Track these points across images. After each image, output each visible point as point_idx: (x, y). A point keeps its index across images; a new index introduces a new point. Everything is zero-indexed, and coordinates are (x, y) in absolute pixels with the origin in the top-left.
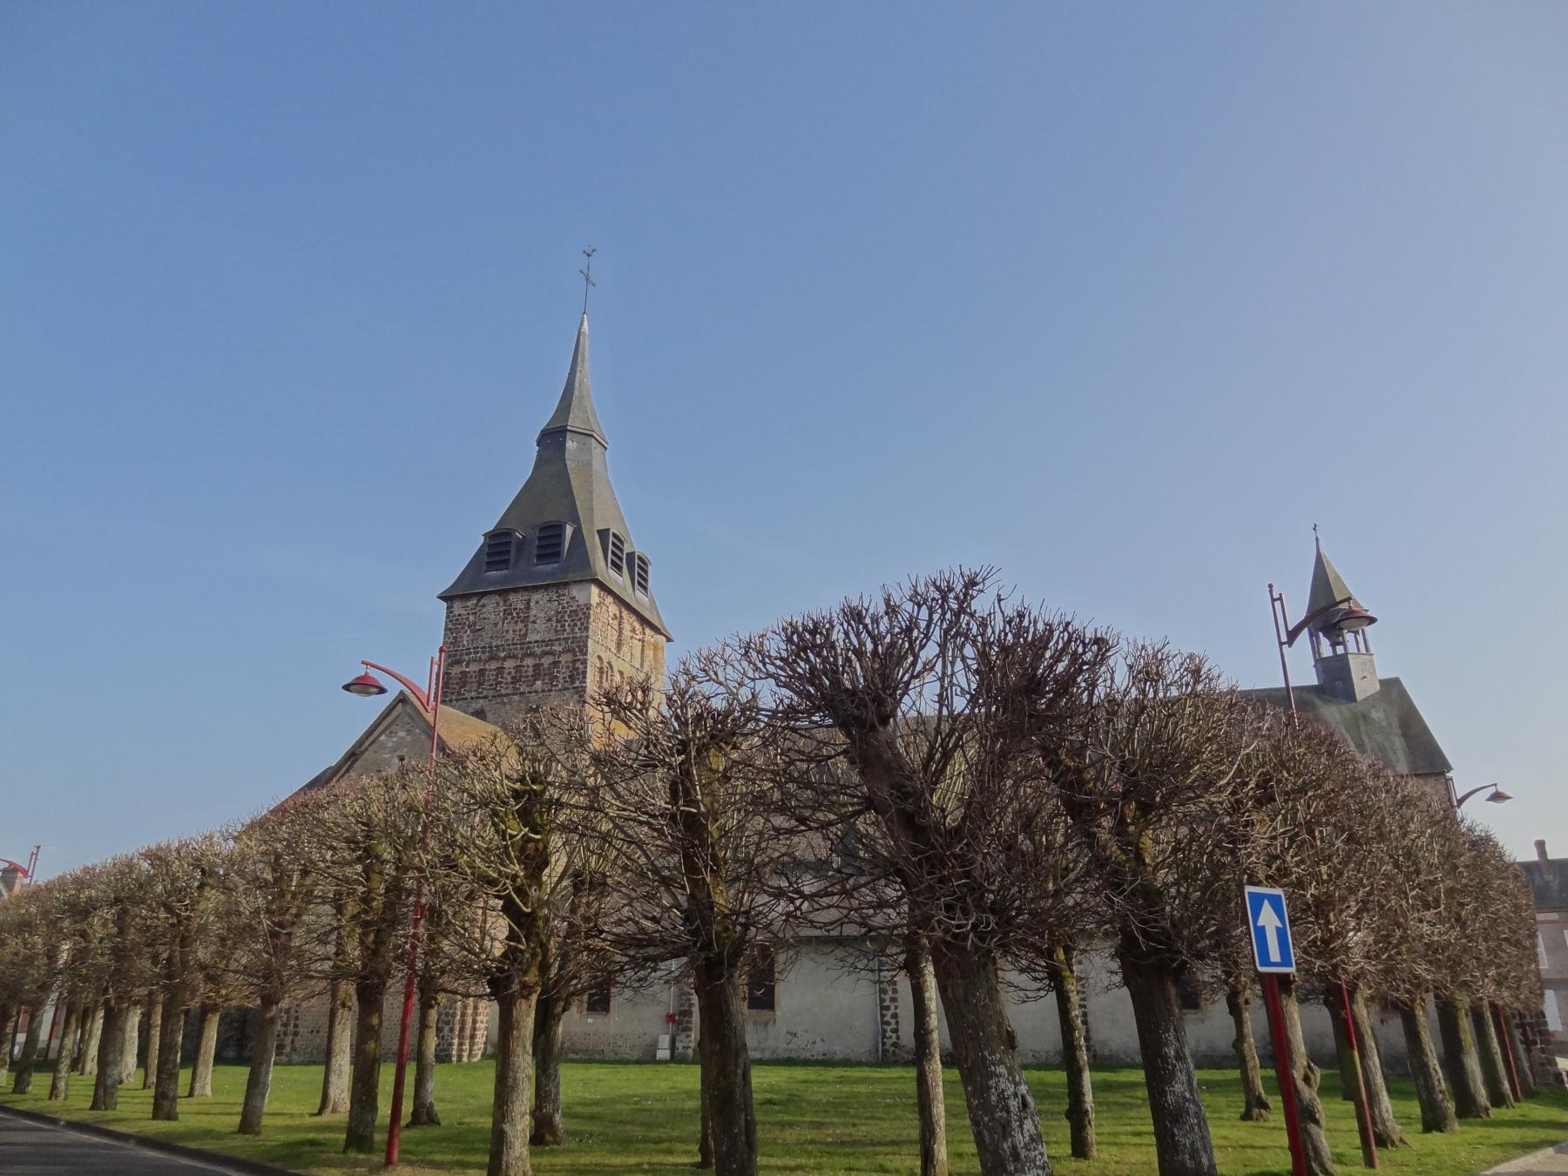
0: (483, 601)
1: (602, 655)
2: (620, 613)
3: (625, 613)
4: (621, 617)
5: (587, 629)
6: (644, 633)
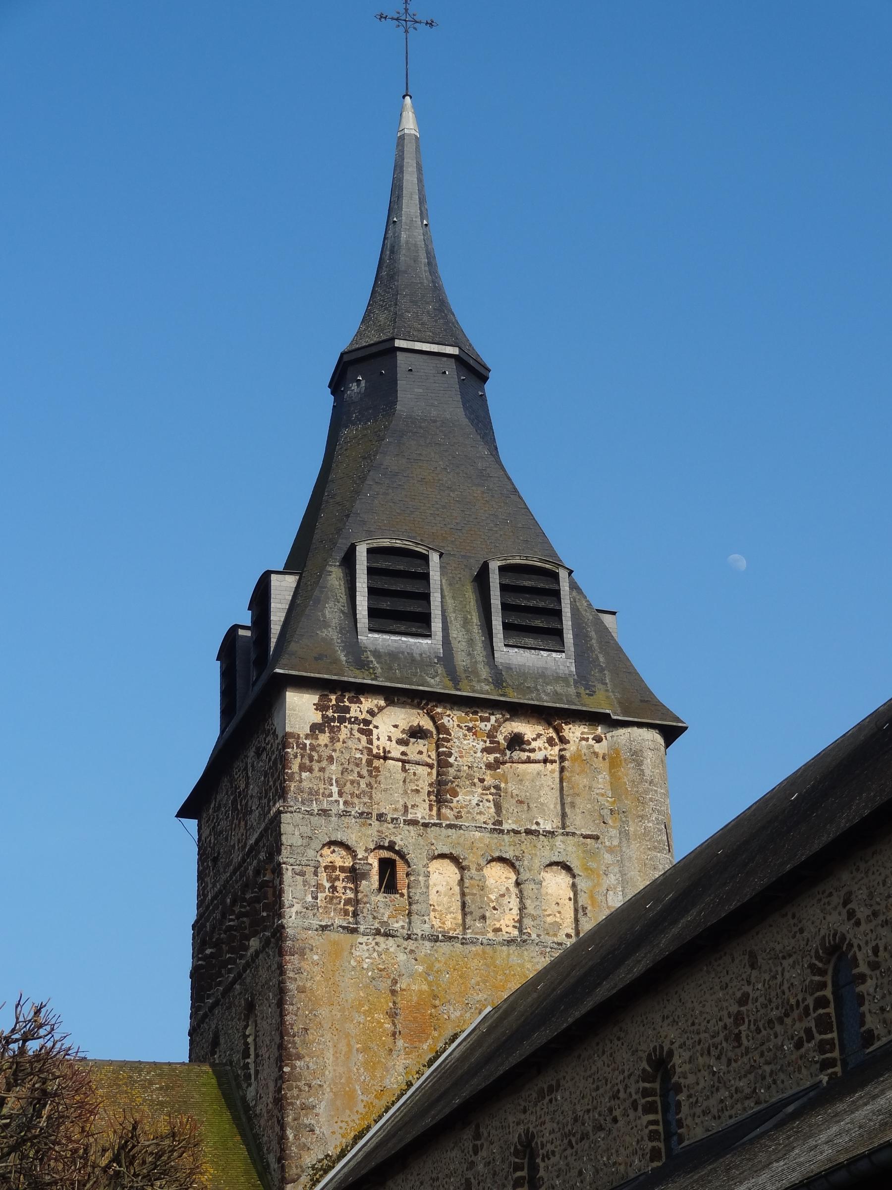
0: (219, 798)
1: (351, 838)
2: (433, 719)
3: (452, 719)
4: (441, 729)
5: (282, 793)
6: (563, 740)
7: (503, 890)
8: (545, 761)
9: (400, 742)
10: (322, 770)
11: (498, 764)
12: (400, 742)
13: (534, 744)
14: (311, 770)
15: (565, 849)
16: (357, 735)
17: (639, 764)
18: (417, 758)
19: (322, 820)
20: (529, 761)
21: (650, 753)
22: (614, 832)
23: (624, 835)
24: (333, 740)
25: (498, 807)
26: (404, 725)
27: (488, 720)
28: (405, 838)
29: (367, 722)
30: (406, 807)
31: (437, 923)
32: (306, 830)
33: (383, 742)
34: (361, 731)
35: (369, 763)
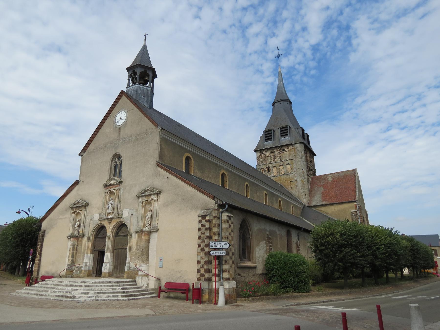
7: (282, 169)
8: (287, 151)
9: (269, 154)
10: (260, 160)
11: (280, 153)
12: (269, 154)
13: (286, 150)
14: (259, 160)
15: (288, 162)
16: (264, 155)
17: (297, 148)
18: (272, 155)
19: (261, 166)
20: (285, 152)
21: (298, 147)
22: (295, 158)
23: (296, 158)
24: (261, 156)
25: (281, 159)
26: (270, 152)
27: (279, 148)
28: (270, 166)
29: (265, 153)
30: (271, 162)
31: (274, 174)
32: (259, 168)
33: (268, 155)
34: (264, 154)
35: (266, 158)
